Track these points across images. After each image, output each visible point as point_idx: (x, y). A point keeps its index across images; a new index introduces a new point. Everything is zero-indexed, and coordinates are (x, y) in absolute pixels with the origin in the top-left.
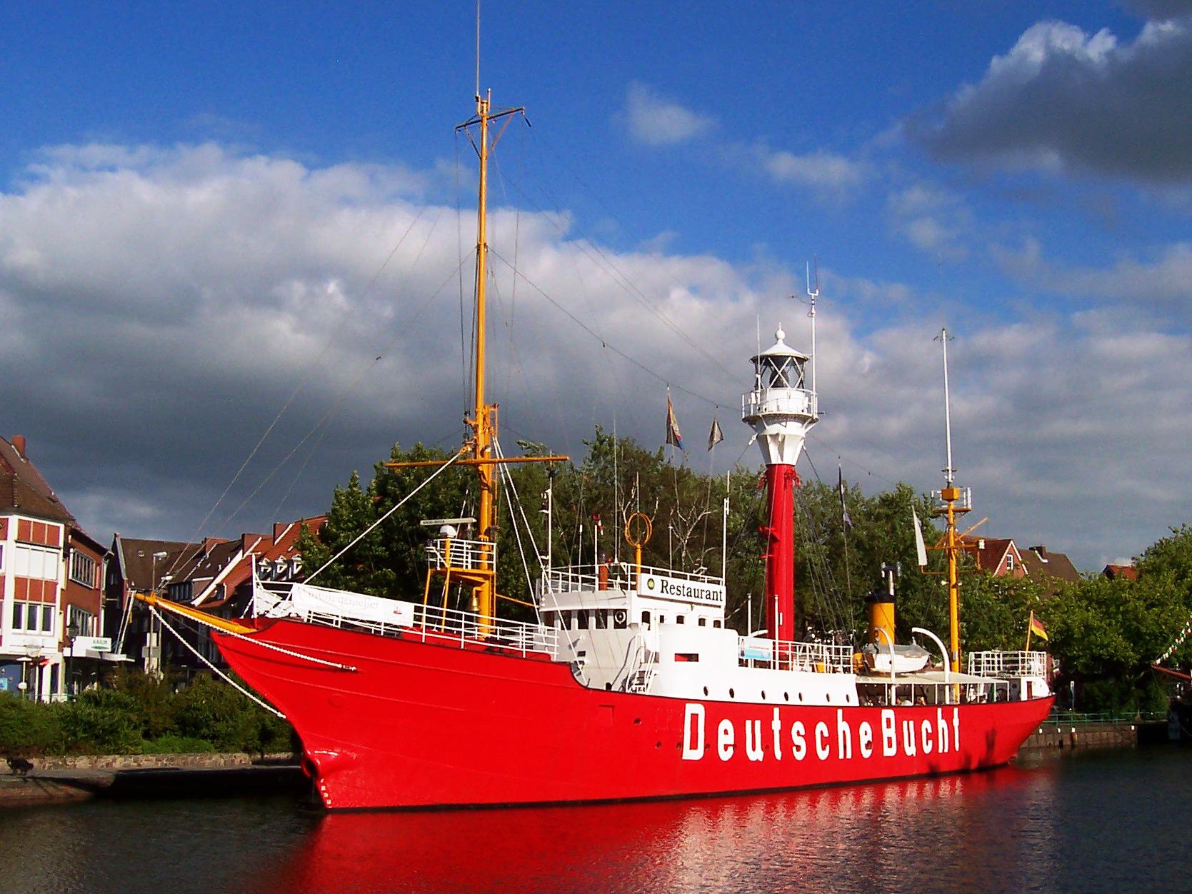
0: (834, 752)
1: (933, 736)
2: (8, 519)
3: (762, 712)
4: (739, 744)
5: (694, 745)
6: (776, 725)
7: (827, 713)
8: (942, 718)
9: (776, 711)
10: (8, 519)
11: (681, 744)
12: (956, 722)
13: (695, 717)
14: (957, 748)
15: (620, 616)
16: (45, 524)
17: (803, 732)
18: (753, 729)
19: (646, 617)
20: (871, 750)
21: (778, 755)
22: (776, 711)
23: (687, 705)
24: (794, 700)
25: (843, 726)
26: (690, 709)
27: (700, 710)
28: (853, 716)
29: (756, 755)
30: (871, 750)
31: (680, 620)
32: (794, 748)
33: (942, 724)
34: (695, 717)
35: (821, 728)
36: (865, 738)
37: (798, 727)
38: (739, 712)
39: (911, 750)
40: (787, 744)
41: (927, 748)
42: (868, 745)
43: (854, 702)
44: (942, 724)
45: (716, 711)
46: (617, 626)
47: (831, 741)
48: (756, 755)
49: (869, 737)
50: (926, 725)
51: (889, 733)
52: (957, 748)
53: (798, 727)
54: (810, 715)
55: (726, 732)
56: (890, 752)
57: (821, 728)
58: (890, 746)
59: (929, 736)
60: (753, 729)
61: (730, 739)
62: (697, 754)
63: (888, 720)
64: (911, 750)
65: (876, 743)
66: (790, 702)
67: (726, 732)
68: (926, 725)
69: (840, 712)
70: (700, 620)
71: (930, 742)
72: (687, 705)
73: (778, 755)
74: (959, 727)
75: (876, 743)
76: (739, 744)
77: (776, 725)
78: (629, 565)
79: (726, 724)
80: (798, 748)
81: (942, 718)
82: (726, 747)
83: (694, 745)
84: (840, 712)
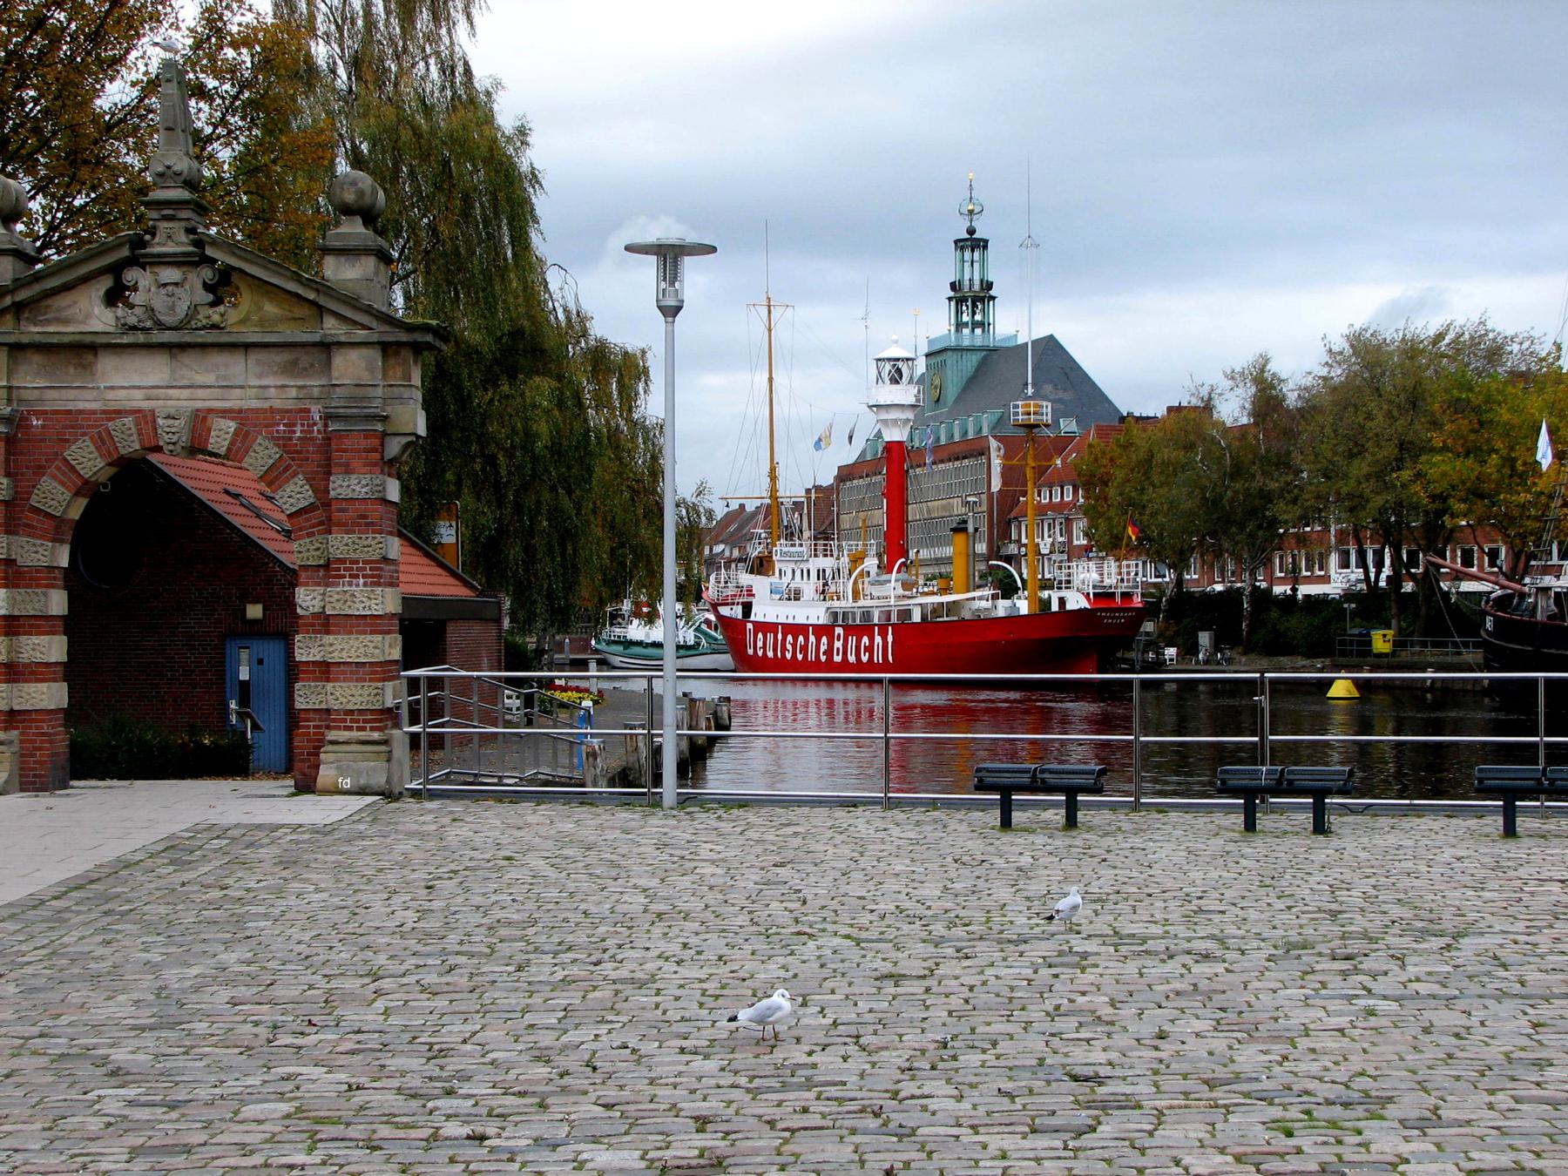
1: (870, 649)
6: (780, 636)
12: (890, 638)
18: (770, 637)
24: (790, 621)
25: (812, 638)
28: (820, 630)
33: (878, 639)
35: (801, 638)
36: (823, 648)
40: (784, 649)
41: (865, 659)
44: (878, 639)
48: (770, 654)
50: (865, 640)
51: (838, 644)
53: (790, 638)
57: (801, 638)
60: (770, 637)
63: (839, 635)
68: (865, 640)
75: (829, 652)
77: (780, 636)
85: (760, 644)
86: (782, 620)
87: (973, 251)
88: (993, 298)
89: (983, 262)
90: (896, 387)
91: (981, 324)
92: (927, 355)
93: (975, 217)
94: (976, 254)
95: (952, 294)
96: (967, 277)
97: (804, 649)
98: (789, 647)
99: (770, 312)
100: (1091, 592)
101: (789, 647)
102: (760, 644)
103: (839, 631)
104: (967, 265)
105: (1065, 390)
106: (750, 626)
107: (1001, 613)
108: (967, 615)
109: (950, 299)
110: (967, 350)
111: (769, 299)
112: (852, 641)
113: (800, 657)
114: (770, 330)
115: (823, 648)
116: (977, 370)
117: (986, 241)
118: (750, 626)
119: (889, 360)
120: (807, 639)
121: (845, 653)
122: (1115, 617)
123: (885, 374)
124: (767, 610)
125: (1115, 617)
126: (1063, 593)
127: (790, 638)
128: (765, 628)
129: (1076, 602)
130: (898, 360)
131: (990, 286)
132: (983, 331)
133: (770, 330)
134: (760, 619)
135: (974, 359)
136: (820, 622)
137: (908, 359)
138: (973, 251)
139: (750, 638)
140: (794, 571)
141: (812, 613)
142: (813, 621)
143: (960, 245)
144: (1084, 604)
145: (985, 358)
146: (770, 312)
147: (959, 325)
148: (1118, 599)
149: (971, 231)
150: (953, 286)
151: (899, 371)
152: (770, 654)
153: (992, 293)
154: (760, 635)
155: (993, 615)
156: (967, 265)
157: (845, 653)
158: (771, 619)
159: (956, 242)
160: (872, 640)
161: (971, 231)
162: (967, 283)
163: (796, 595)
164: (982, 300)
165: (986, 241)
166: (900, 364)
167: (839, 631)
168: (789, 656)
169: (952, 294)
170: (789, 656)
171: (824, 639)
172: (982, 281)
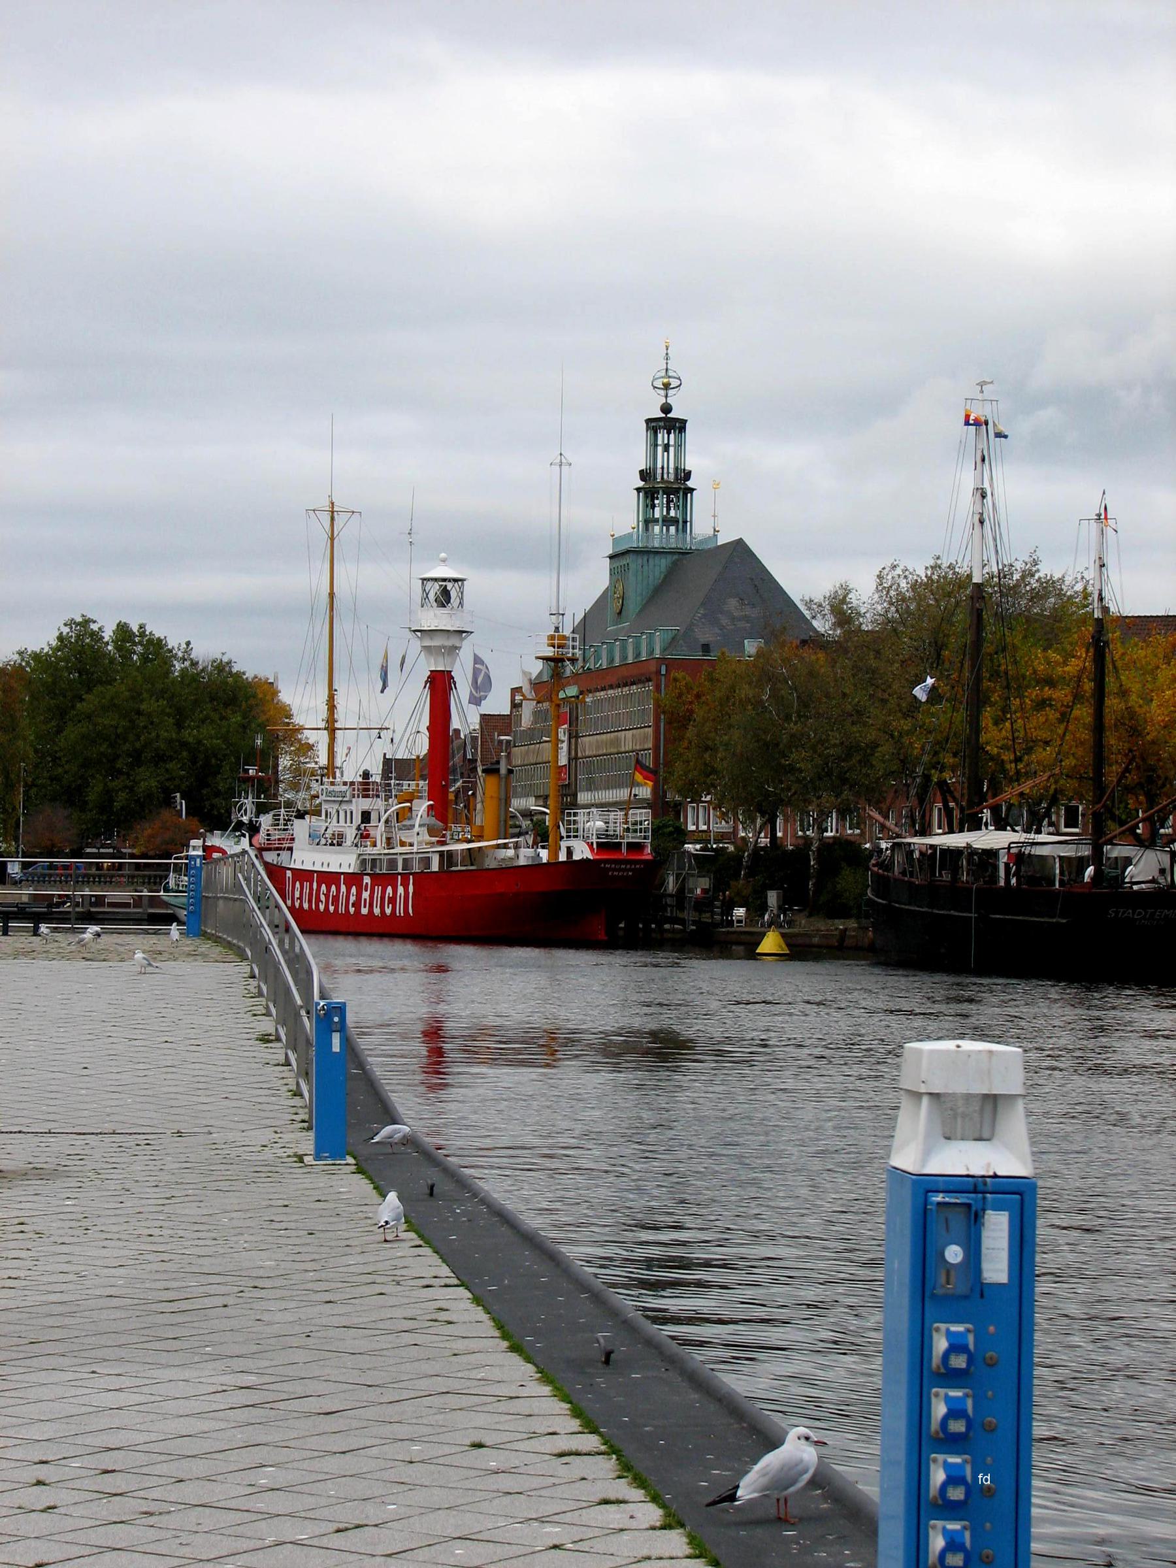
1: (393, 900)
18: (307, 885)
24: (325, 869)
25: (343, 888)
33: (401, 890)
35: (333, 888)
36: (352, 899)
39: (377, 911)
40: (318, 900)
41: (388, 911)
42: (353, 905)
44: (401, 890)
48: (306, 906)
50: (389, 890)
51: (366, 895)
53: (324, 887)
57: (333, 888)
65: (357, 905)
68: (389, 890)
75: (357, 905)
76: (301, 898)
85: (297, 894)
86: (318, 868)
87: (669, 433)
88: (692, 490)
89: (680, 446)
90: (442, 610)
91: (674, 521)
92: (611, 557)
93: (671, 392)
94: (672, 436)
95: (641, 484)
96: (659, 465)
97: (336, 899)
98: (323, 898)
99: (332, 519)
100: (595, 840)
101: (323, 898)
102: (297, 894)
103: (367, 880)
104: (660, 449)
105: (754, 606)
106: (289, 874)
107: (522, 862)
108: (491, 864)
109: (638, 490)
110: (656, 553)
111: (333, 504)
112: (378, 890)
113: (332, 908)
114: (332, 539)
115: (352, 899)
116: (666, 577)
117: (684, 422)
118: (289, 874)
119: (436, 580)
122: (620, 870)
123: (432, 596)
124: (306, 857)
125: (620, 870)
126: (570, 843)
127: (324, 887)
128: (303, 875)
129: (582, 851)
130: (444, 580)
131: (688, 475)
132: (677, 530)
133: (332, 539)
135: (663, 563)
136: (351, 871)
137: (456, 580)
138: (669, 433)
139: (288, 888)
140: (338, 812)
141: (344, 861)
142: (345, 869)
143: (653, 425)
144: (588, 855)
145: (675, 563)
146: (332, 519)
147: (648, 522)
148: (624, 849)
149: (666, 409)
150: (644, 475)
151: (446, 593)
152: (306, 906)
153: (690, 484)
154: (298, 883)
155: (516, 864)
156: (660, 449)
158: (308, 866)
159: (648, 421)
160: (395, 891)
161: (666, 409)
162: (659, 471)
163: (337, 841)
164: (676, 491)
165: (684, 422)
166: (449, 586)
167: (367, 880)
168: (322, 907)
169: (641, 484)
170: (322, 907)
171: (354, 890)
172: (676, 469)
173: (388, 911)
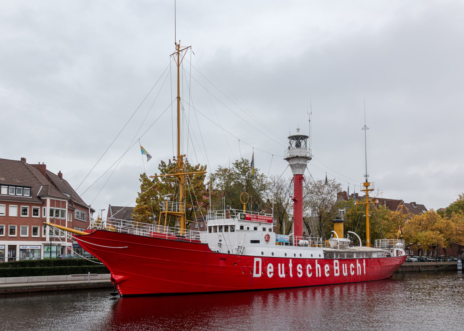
0: (314, 274)
1: (355, 269)
2: (46, 199)
3: (285, 261)
4: (276, 271)
5: (257, 272)
6: (291, 265)
7: (312, 261)
8: (318, 264)
9: (291, 260)
10: (46, 199)
11: (252, 272)
12: (364, 264)
13: (258, 263)
14: (365, 272)
15: (233, 227)
16: (60, 201)
17: (301, 268)
19: (242, 228)
20: (329, 274)
21: (291, 275)
22: (291, 260)
23: (255, 258)
24: (298, 256)
25: (318, 266)
26: (256, 260)
27: (260, 260)
28: (322, 262)
29: (283, 275)
30: (329, 274)
31: (255, 229)
32: (298, 273)
33: (358, 265)
34: (258, 263)
35: (309, 266)
37: (299, 266)
38: (275, 261)
39: (345, 274)
40: (295, 271)
41: (352, 273)
42: (328, 272)
43: (323, 257)
44: (358, 265)
45: (266, 260)
46: (231, 231)
47: (313, 271)
48: (283, 275)
49: (328, 269)
51: (336, 268)
52: (365, 272)
54: (304, 262)
55: (270, 268)
56: (337, 275)
57: (309, 266)
58: (337, 272)
59: (353, 269)
61: (272, 270)
62: (259, 275)
64: (345, 274)
65: (331, 271)
66: (296, 257)
67: (270, 268)
68: (352, 265)
69: (316, 261)
70: (263, 229)
71: (354, 271)
72: (255, 258)
73: (291, 275)
74: (292, 267)
75: (331, 271)
76: (276, 271)
77: (291, 265)
78: (235, 210)
79: (299, 266)
80: (300, 273)
81: (318, 264)
82: (270, 273)
83: (257, 272)
84: (316, 261)
115: (326, 270)
120: (313, 266)
121: (341, 271)
134: (268, 254)
157: (341, 271)
173: (352, 273)
